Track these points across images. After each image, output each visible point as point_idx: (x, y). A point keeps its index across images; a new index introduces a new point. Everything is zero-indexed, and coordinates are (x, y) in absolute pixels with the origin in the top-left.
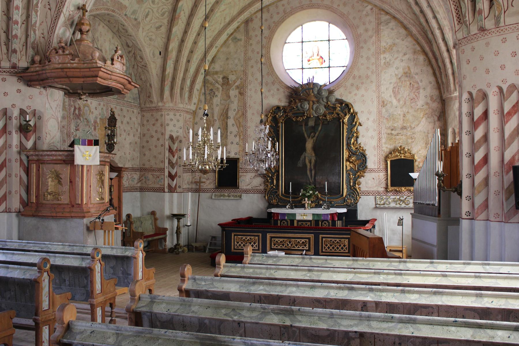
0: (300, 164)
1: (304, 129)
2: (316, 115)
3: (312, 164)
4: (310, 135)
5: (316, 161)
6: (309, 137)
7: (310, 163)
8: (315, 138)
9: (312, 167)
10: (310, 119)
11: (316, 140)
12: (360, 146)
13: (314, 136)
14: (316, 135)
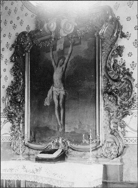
0: (47, 103)
1: (51, 56)
2: (66, 35)
3: (61, 101)
4: (58, 62)
5: (65, 96)
6: (57, 66)
7: (59, 99)
8: (64, 66)
9: (61, 105)
10: (58, 42)
11: (66, 67)
12: (124, 68)
13: (63, 63)
14: (66, 61)
